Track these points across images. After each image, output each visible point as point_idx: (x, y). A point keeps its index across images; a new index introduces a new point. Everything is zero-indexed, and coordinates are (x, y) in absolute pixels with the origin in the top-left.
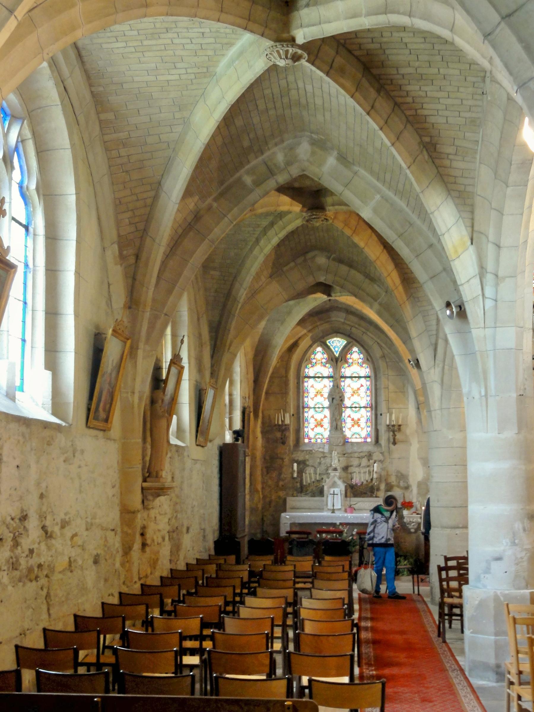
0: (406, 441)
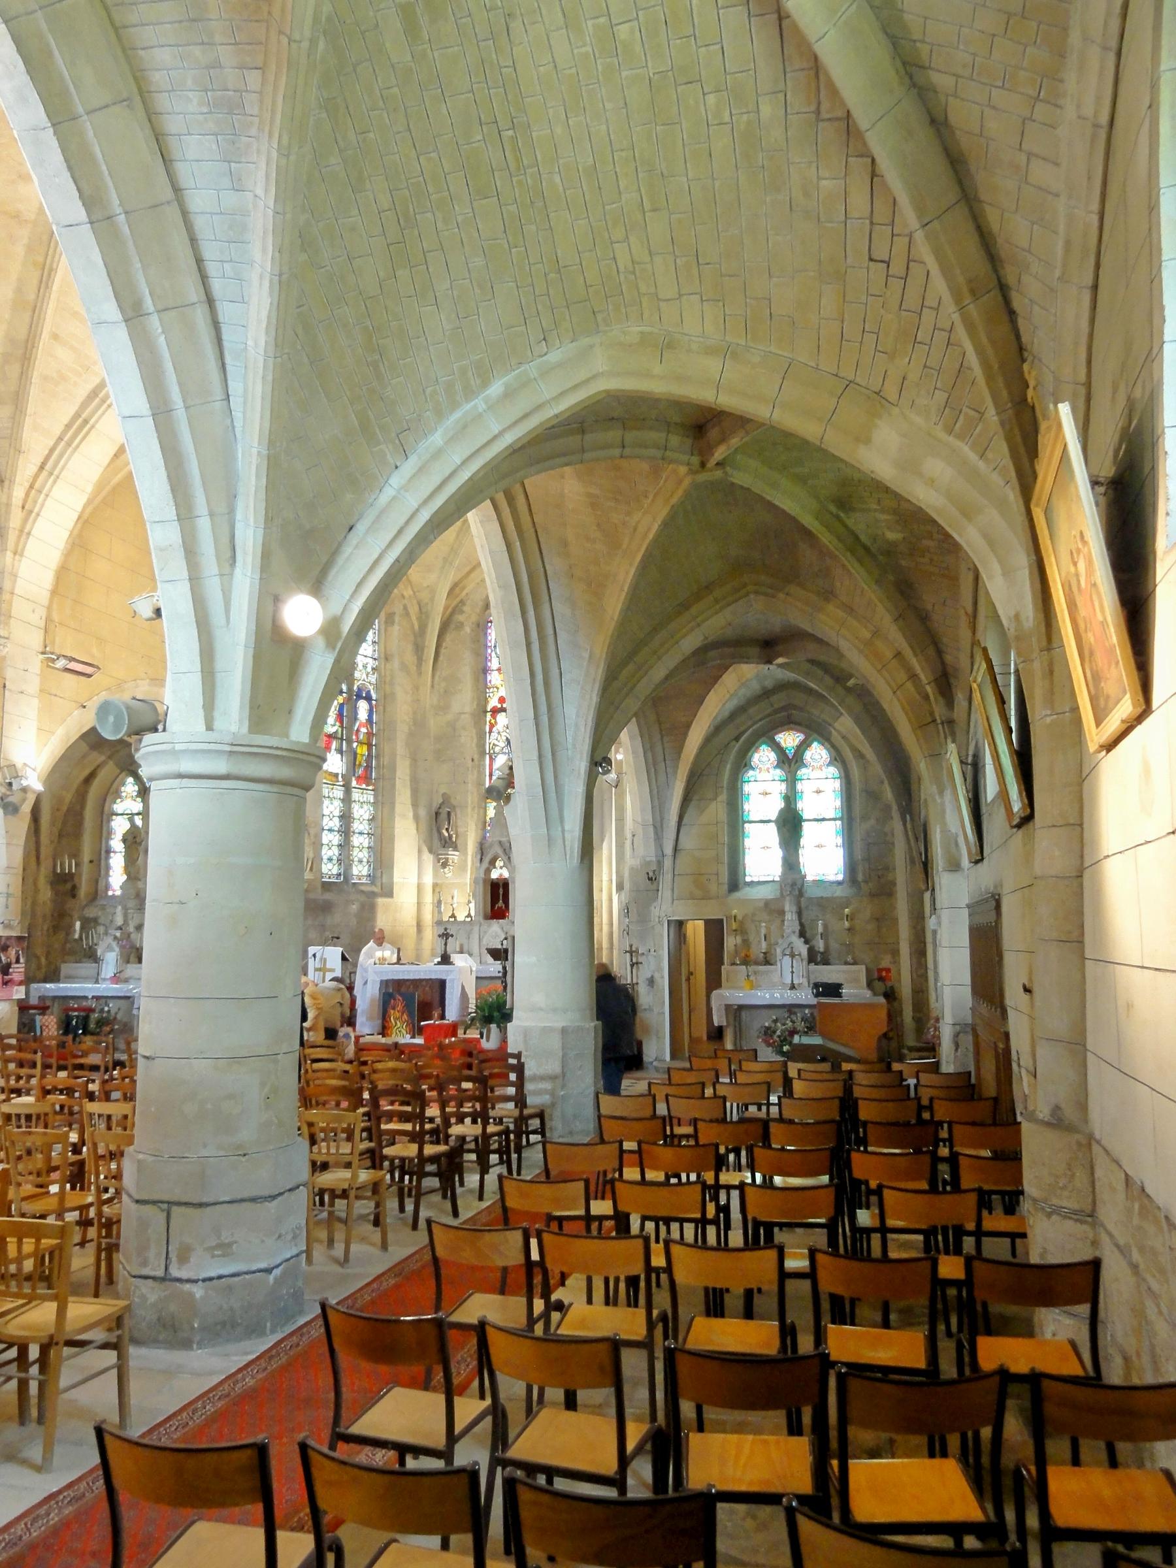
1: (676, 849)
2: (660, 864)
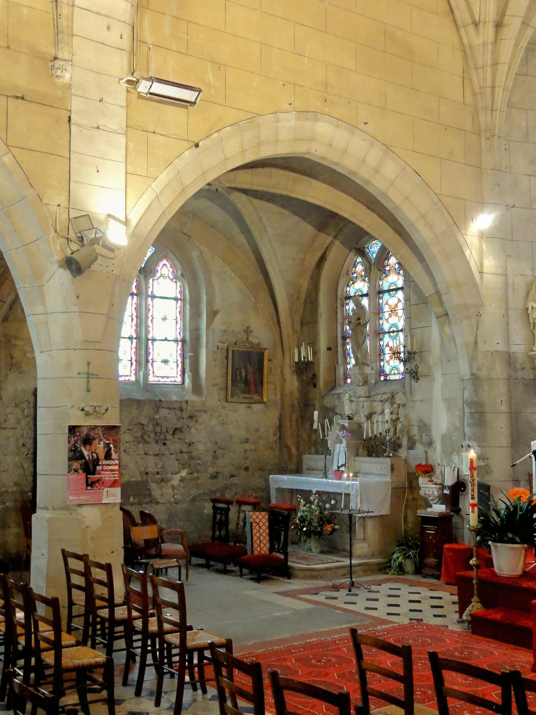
0: (429, 375)
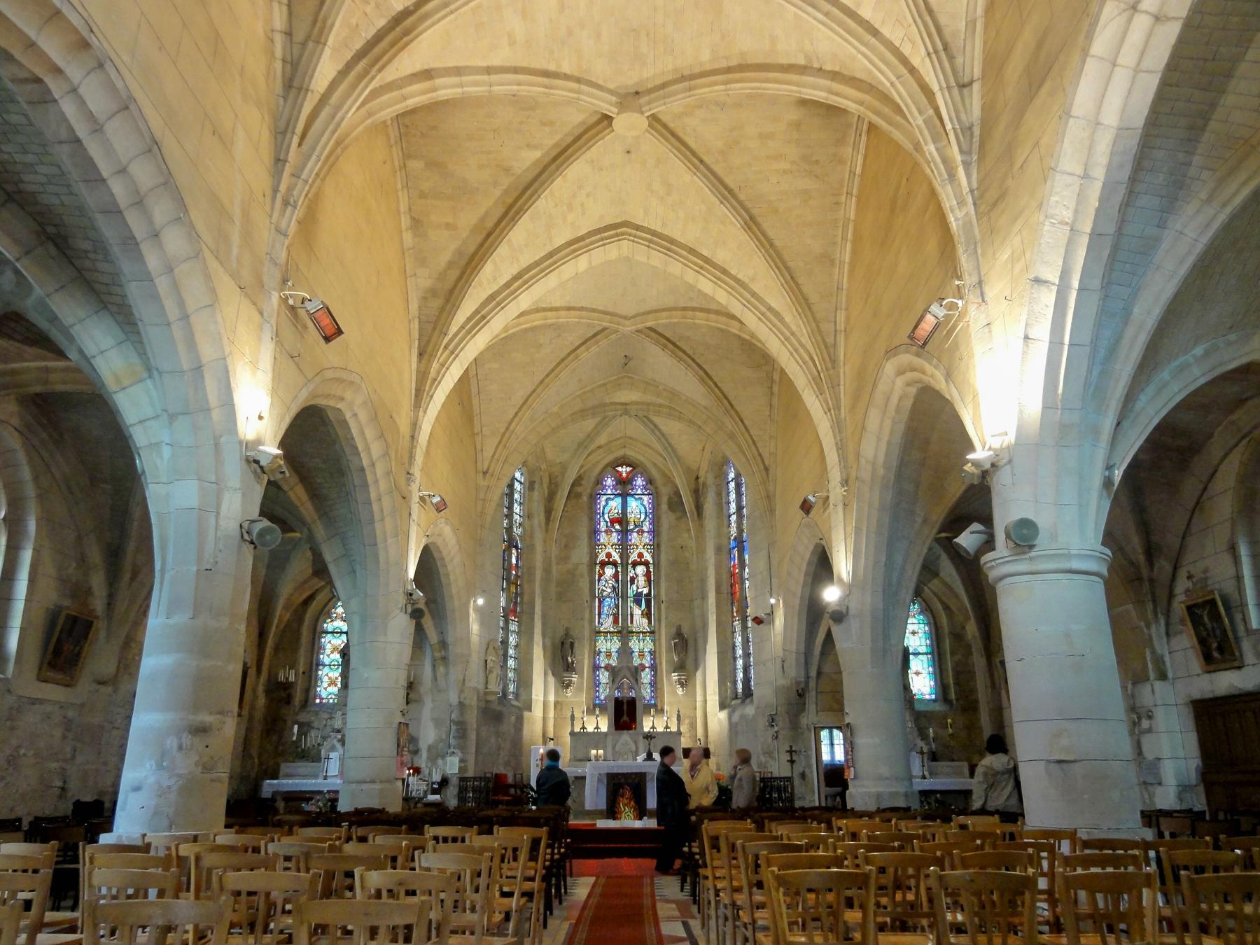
0: (419, 701)
1: (819, 673)
2: (807, 683)
